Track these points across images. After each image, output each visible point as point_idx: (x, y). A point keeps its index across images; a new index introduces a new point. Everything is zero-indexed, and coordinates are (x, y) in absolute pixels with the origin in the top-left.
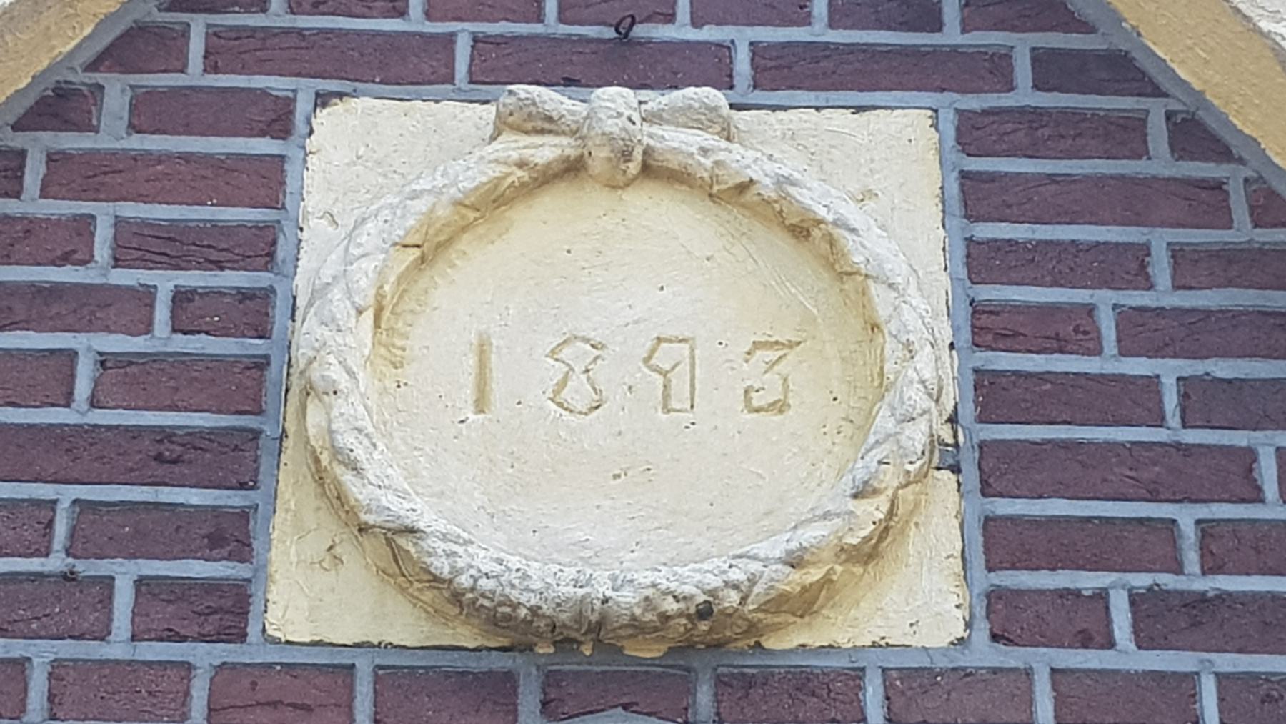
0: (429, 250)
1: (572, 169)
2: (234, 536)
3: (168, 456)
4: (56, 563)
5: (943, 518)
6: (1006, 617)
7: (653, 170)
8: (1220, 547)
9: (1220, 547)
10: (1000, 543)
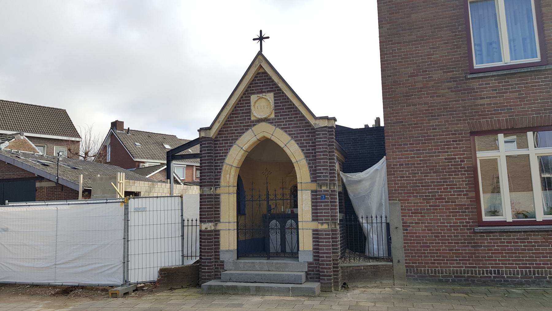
0: (255, 103)
2: (250, 116)
5: (273, 113)
6: (276, 116)
8: (283, 112)
9: (283, 112)
10: (275, 113)
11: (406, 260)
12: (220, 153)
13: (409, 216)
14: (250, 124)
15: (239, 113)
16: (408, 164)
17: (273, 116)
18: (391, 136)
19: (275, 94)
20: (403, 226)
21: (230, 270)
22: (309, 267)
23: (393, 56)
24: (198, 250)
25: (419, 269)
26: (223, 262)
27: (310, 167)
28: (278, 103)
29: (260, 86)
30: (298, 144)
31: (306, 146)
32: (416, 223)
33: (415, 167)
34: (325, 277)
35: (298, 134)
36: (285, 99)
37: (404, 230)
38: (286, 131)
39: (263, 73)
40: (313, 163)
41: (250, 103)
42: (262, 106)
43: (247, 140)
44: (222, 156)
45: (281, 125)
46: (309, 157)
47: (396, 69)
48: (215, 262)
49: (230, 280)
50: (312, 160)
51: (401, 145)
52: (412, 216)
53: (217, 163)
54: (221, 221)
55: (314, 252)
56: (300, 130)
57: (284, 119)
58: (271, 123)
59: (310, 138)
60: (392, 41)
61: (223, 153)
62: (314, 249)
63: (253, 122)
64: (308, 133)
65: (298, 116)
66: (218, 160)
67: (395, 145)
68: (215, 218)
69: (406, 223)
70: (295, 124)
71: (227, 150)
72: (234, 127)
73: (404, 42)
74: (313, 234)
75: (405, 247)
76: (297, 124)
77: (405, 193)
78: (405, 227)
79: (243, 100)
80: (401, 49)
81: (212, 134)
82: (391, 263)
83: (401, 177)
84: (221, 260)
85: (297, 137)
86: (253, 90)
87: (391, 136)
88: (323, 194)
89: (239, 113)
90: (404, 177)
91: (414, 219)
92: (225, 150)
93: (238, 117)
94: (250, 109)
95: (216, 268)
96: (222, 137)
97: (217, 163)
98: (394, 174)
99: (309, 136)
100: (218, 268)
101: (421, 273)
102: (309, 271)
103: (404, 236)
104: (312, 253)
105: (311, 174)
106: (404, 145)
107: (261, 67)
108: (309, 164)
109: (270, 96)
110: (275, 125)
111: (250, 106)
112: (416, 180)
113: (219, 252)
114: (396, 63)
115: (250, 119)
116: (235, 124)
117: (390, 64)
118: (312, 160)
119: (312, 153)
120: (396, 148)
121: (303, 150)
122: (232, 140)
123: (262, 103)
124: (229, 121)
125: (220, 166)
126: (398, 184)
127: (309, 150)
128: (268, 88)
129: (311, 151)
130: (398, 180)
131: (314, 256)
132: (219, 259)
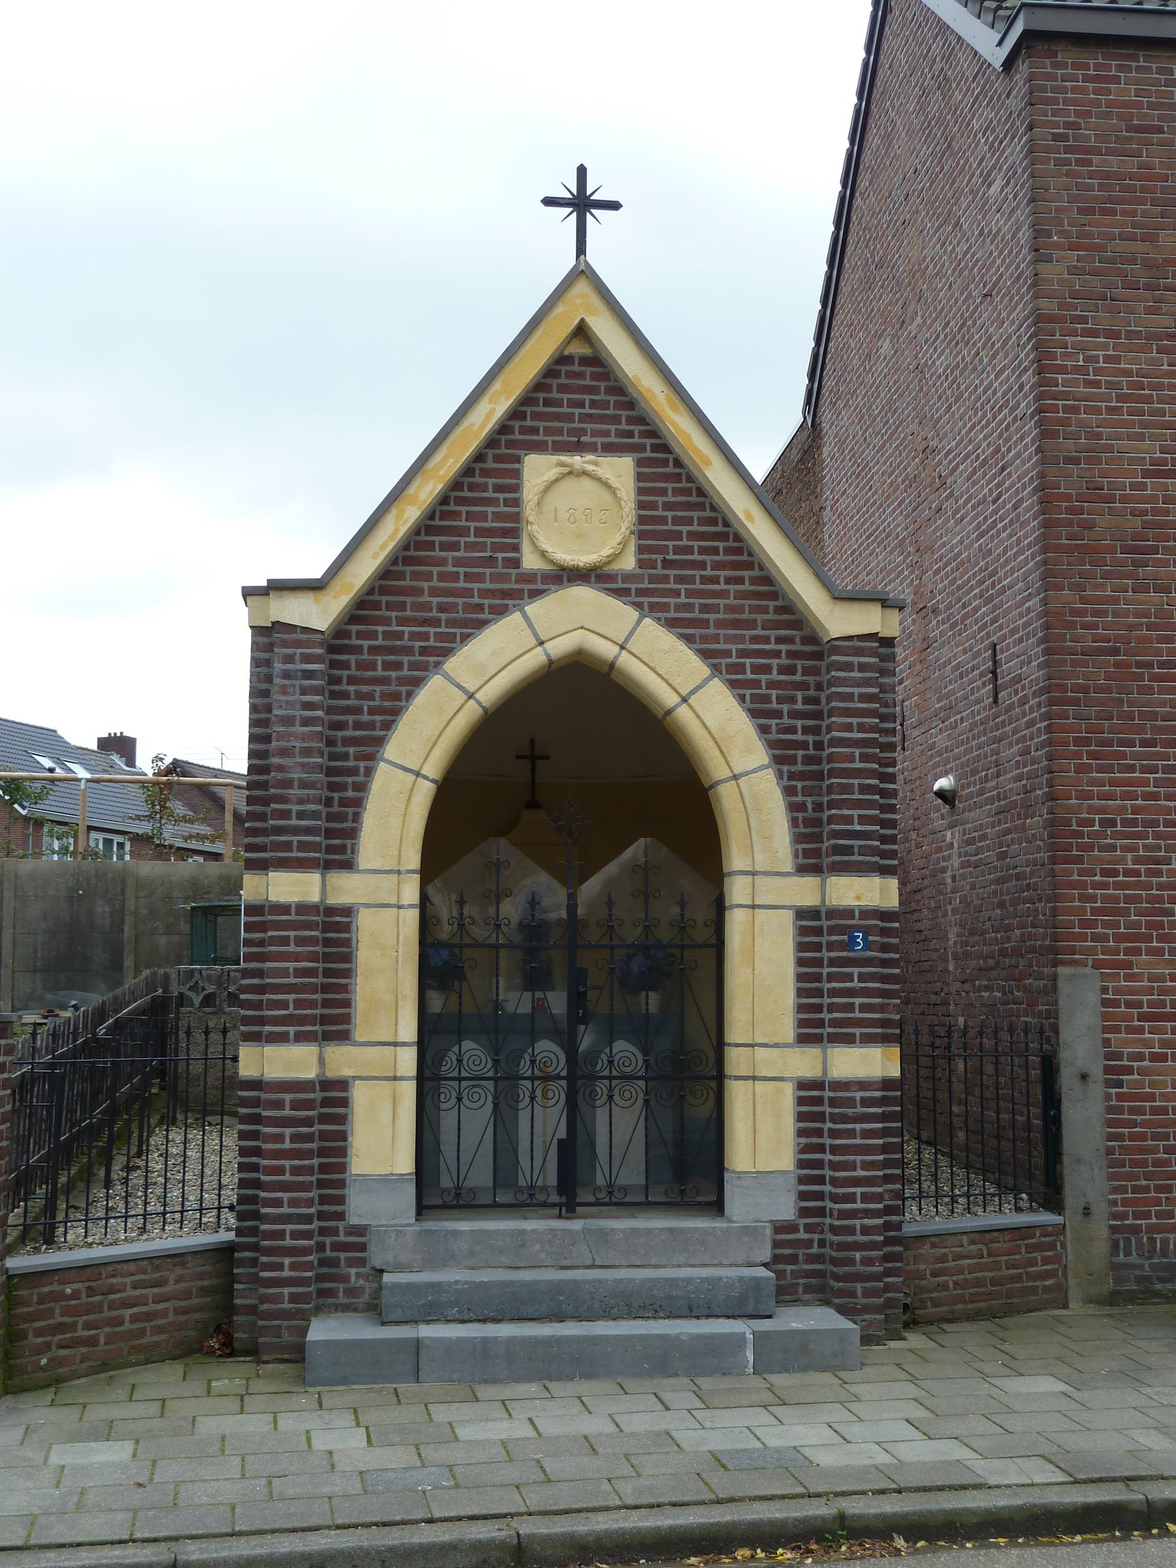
1: (570, 473)
2: (516, 548)
3: (505, 533)
4: (488, 554)
5: (632, 547)
7: (584, 473)
9: (677, 550)
10: (641, 549)
11: (1114, 1203)
12: (358, 711)
13: (1131, 1030)
14: (518, 588)
15: (464, 532)
16: (1134, 823)
17: (629, 563)
18: (1075, 702)
19: (639, 463)
20: (1108, 1070)
21: (400, 1268)
22: (776, 1244)
23: (1088, 383)
24: (231, 1178)
25: (1158, 1236)
26: (361, 1230)
27: (793, 808)
28: (652, 506)
29: (569, 418)
30: (742, 699)
31: (778, 714)
32: (1155, 1057)
33: (1158, 835)
34: (866, 1277)
35: (743, 654)
36: (686, 492)
37: (1109, 1084)
38: (688, 639)
39: (584, 361)
40: (807, 792)
41: (517, 488)
42: (578, 507)
43: (495, 660)
44: (370, 726)
45: (664, 607)
46: (792, 760)
47: (1099, 436)
48: (323, 1231)
49: (431, 1313)
50: (802, 776)
51: (1108, 743)
52: (1141, 1030)
53: (345, 757)
54: (359, 1035)
55: (802, 1180)
56: (755, 639)
57: (680, 579)
58: (619, 593)
59: (798, 677)
60: (1084, 319)
61: (372, 712)
62: (801, 1164)
63: (530, 577)
64: (791, 655)
65: (746, 574)
66: (347, 742)
67: (1086, 742)
68: (324, 1020)
69: (1118, 1056)
70: (730, 609)
71: (396, 696)
72: (433, 592)
73: (1130, 335)
74: (801, 1101)
75: (1110, 1151)
76: (740, 609)
77: (1119, 938)
78: (1114, 1073)
79: (486, 473)
80: (1116, 359)
81: (318, 614)
82: (1058, 1219)
83: (1106, 873)
84: (354, 1220)
85: (740, 668)
86: (535, 431)
87: (1075, 702)
88: (858, 928)
89: (464, 532)
90: (1115, 873)
91: (1148, 1044)
92: (384, 696)
93: (455, 547)
94: (516, 517)
95: (323, 1262)
96: (373, 635)
97: (345, 757)
98: (1079, 860)
99: (791, 670)
100: (335, 1263)
101: (1164, 1253)
102: (776, 1259)
103: (1110, 1110)
104: (793, 1181)
105: (798, 838)
106: (1122, 743)
107: (582, 331)
108: (789, 791)
109: (620, 471)
110: (638, 606)
111: (516, 503)
112: (1161, 887)
113: (342, 1184)
114: (1098, 411)
115: (516, 563)
116: (442, 577)
117: (1075, 410)
118: (802, 776)
119: (804, 745)
120: (1092, 755)
121: (763, 730)
122: (424, 651)
123: (580, 493)
124: (407, 561)
125: (354, 772)
126: (1093, 898)
127: (792, 730)
128: (607, 434)
129: (799, 737)
130: (1096, 885)
131: (803, 1196)
132: (341, 1216)
